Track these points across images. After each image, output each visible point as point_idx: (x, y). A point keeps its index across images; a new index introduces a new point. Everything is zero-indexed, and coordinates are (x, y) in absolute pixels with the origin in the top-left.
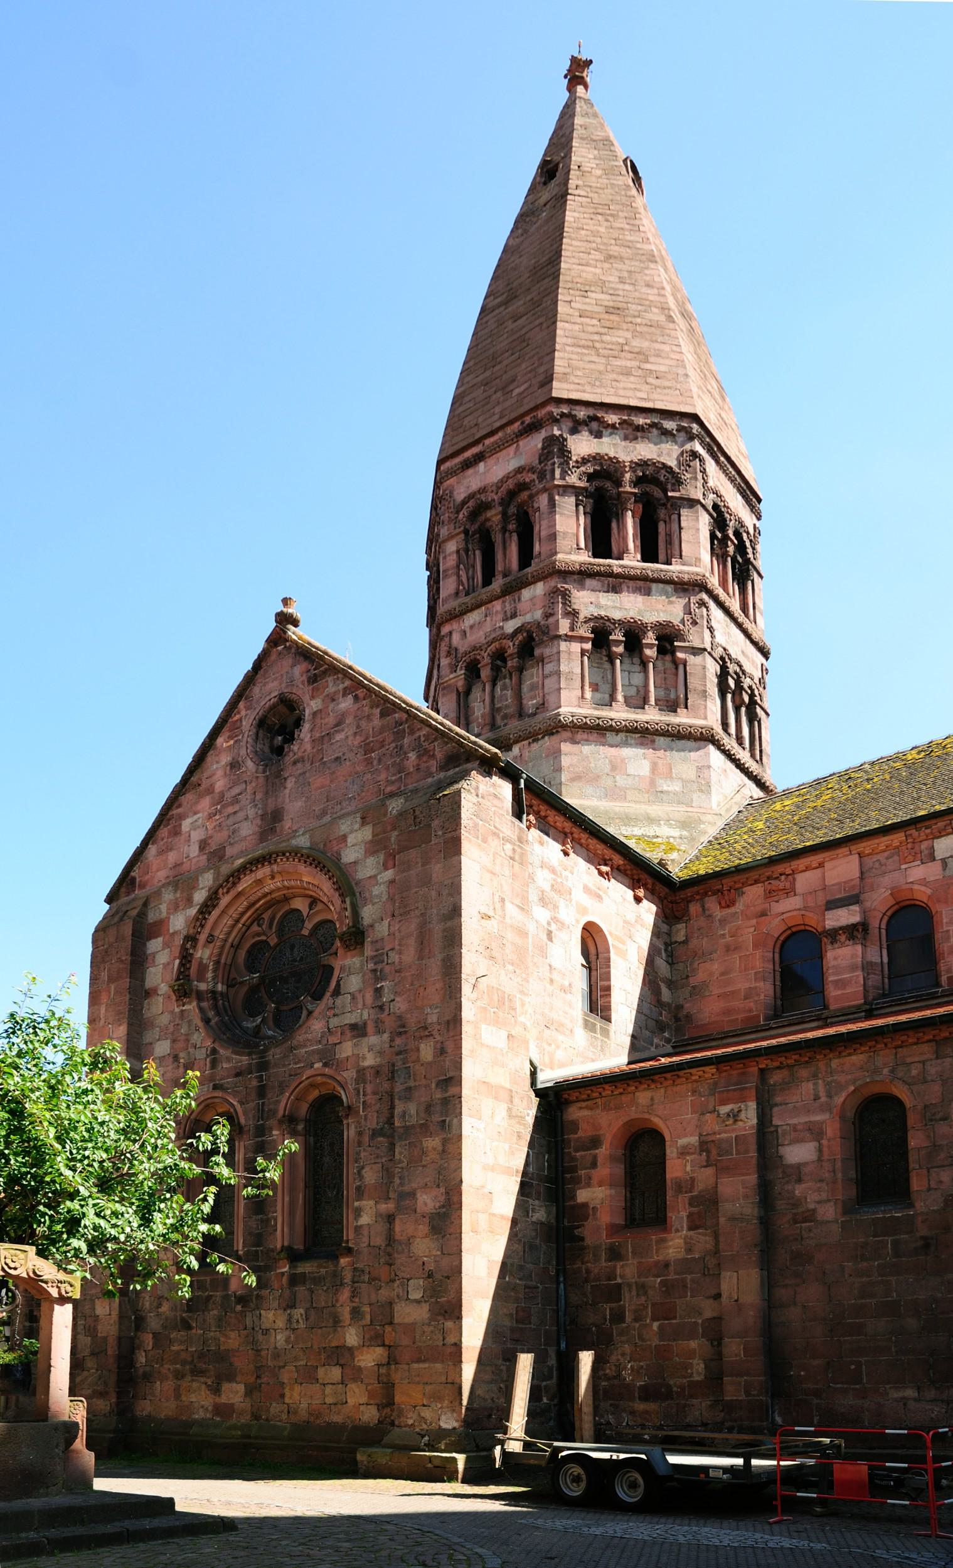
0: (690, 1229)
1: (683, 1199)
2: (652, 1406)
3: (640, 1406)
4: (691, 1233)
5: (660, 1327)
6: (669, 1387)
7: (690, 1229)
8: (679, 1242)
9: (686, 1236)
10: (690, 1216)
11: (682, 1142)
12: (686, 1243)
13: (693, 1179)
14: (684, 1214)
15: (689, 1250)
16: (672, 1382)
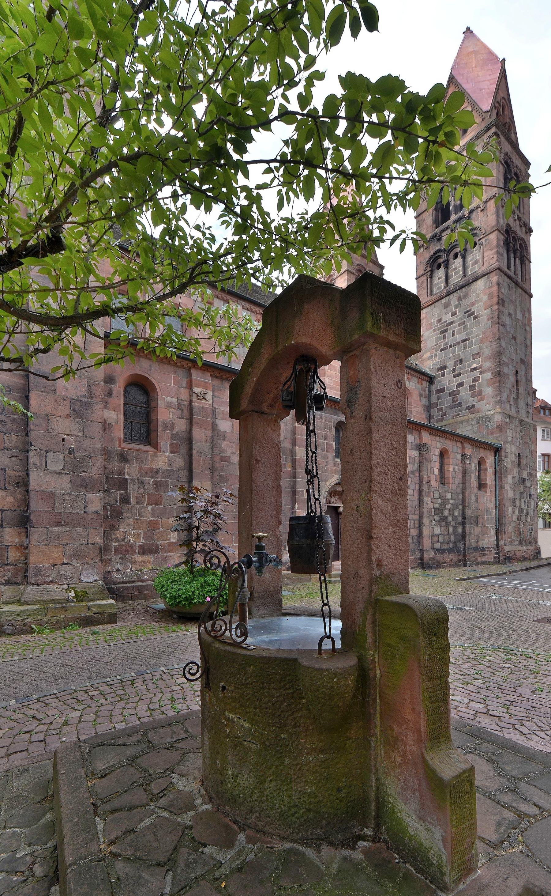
0: (171, 452)
1: (168, 434)
2: (147, 558)
3: (139, 558)
4: (171, 455)
5: (152, 509)
6: (157, 546)
7: (171, 452)
8: (164, 459)
9: (169, 457)
10: (171, 444)
11: (168, 399)
12: (168, 460)
13: (173, 424)
14: (168, 443)
15: (170, 465)
16: (158, 543)
